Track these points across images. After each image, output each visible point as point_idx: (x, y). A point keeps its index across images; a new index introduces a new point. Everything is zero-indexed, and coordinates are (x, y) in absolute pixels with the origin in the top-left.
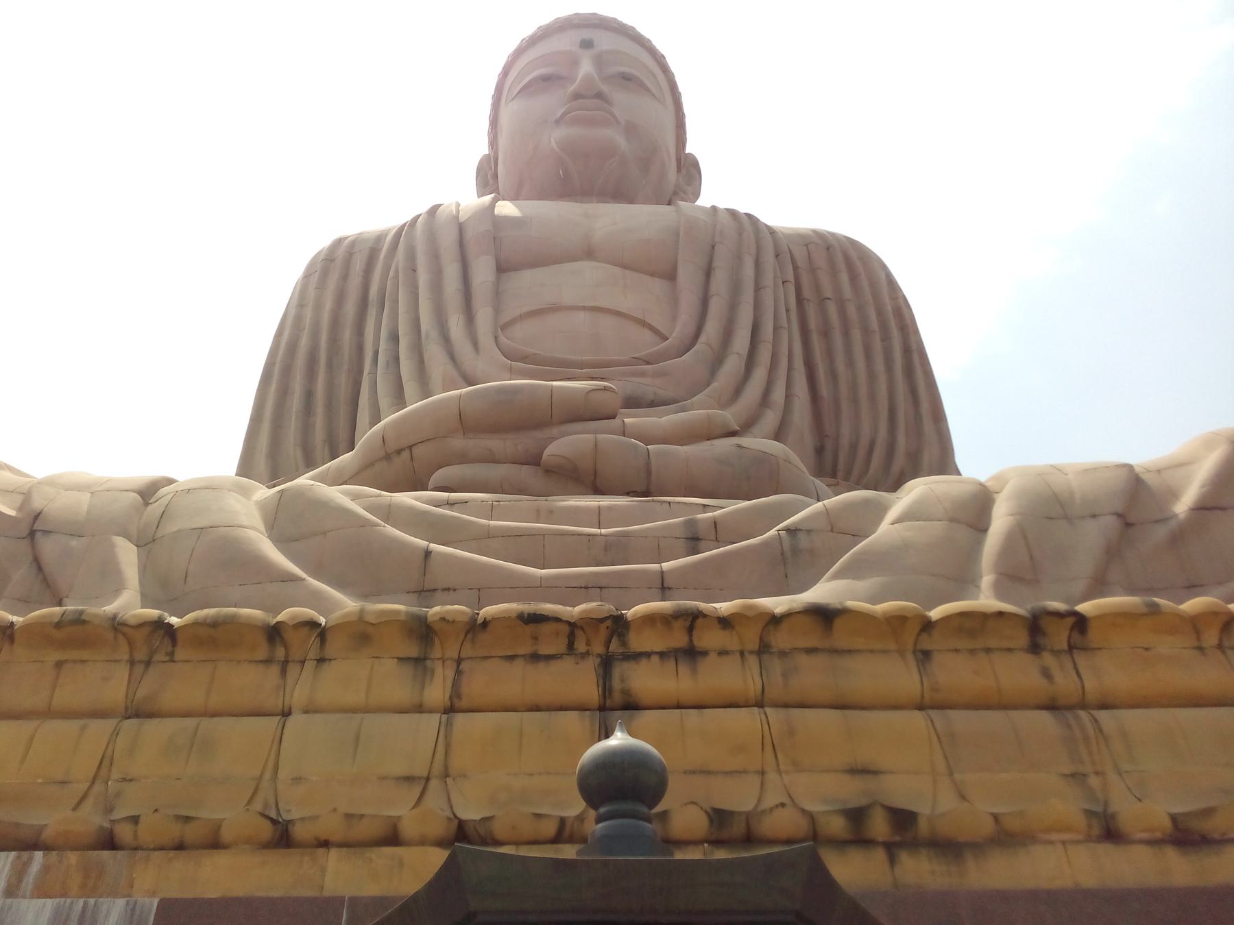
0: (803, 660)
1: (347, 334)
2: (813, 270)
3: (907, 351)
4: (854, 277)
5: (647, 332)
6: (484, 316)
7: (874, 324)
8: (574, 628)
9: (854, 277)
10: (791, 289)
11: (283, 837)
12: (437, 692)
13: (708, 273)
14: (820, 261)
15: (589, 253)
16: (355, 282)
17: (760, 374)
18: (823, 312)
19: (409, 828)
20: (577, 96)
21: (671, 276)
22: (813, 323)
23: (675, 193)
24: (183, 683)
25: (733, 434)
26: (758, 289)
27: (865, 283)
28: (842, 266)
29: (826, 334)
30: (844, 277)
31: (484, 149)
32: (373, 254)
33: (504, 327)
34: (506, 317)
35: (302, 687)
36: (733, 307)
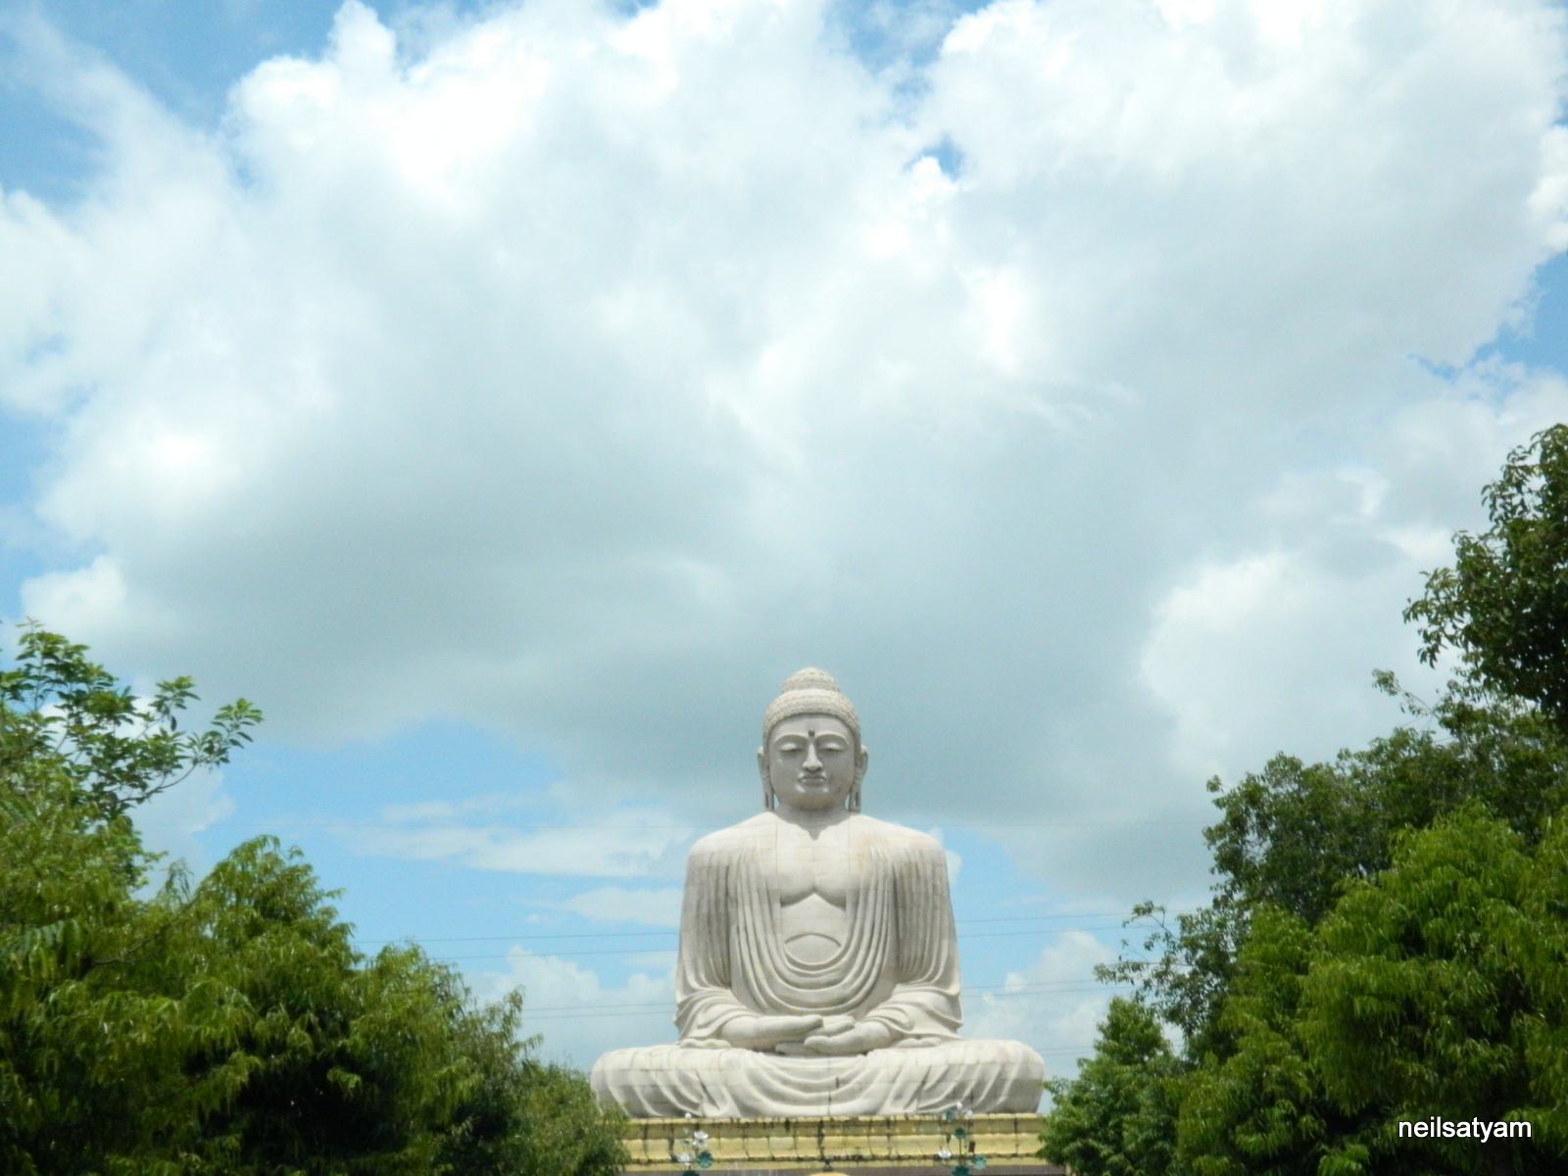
1: (722, 909)
2: (902, 877)
3: (935, 908)
4: (918, 877)
5: (834, 944)
6: (779, 935)
7: (922, 902)
9: (918, 877)
10: (891, 894)
11: (773, 1159)
14: (904, 872)
15: (814, 890)
16: (722, 882)
18: (904, 899)
22: (900, 905)
23: (854, 783)
27: (922, 879)
28: (914, 874)
29: (904, 908)
30: (914, 880)
32: (728, 868)
33: (787, 941)
34: (787, 938)
36: (864, 919)
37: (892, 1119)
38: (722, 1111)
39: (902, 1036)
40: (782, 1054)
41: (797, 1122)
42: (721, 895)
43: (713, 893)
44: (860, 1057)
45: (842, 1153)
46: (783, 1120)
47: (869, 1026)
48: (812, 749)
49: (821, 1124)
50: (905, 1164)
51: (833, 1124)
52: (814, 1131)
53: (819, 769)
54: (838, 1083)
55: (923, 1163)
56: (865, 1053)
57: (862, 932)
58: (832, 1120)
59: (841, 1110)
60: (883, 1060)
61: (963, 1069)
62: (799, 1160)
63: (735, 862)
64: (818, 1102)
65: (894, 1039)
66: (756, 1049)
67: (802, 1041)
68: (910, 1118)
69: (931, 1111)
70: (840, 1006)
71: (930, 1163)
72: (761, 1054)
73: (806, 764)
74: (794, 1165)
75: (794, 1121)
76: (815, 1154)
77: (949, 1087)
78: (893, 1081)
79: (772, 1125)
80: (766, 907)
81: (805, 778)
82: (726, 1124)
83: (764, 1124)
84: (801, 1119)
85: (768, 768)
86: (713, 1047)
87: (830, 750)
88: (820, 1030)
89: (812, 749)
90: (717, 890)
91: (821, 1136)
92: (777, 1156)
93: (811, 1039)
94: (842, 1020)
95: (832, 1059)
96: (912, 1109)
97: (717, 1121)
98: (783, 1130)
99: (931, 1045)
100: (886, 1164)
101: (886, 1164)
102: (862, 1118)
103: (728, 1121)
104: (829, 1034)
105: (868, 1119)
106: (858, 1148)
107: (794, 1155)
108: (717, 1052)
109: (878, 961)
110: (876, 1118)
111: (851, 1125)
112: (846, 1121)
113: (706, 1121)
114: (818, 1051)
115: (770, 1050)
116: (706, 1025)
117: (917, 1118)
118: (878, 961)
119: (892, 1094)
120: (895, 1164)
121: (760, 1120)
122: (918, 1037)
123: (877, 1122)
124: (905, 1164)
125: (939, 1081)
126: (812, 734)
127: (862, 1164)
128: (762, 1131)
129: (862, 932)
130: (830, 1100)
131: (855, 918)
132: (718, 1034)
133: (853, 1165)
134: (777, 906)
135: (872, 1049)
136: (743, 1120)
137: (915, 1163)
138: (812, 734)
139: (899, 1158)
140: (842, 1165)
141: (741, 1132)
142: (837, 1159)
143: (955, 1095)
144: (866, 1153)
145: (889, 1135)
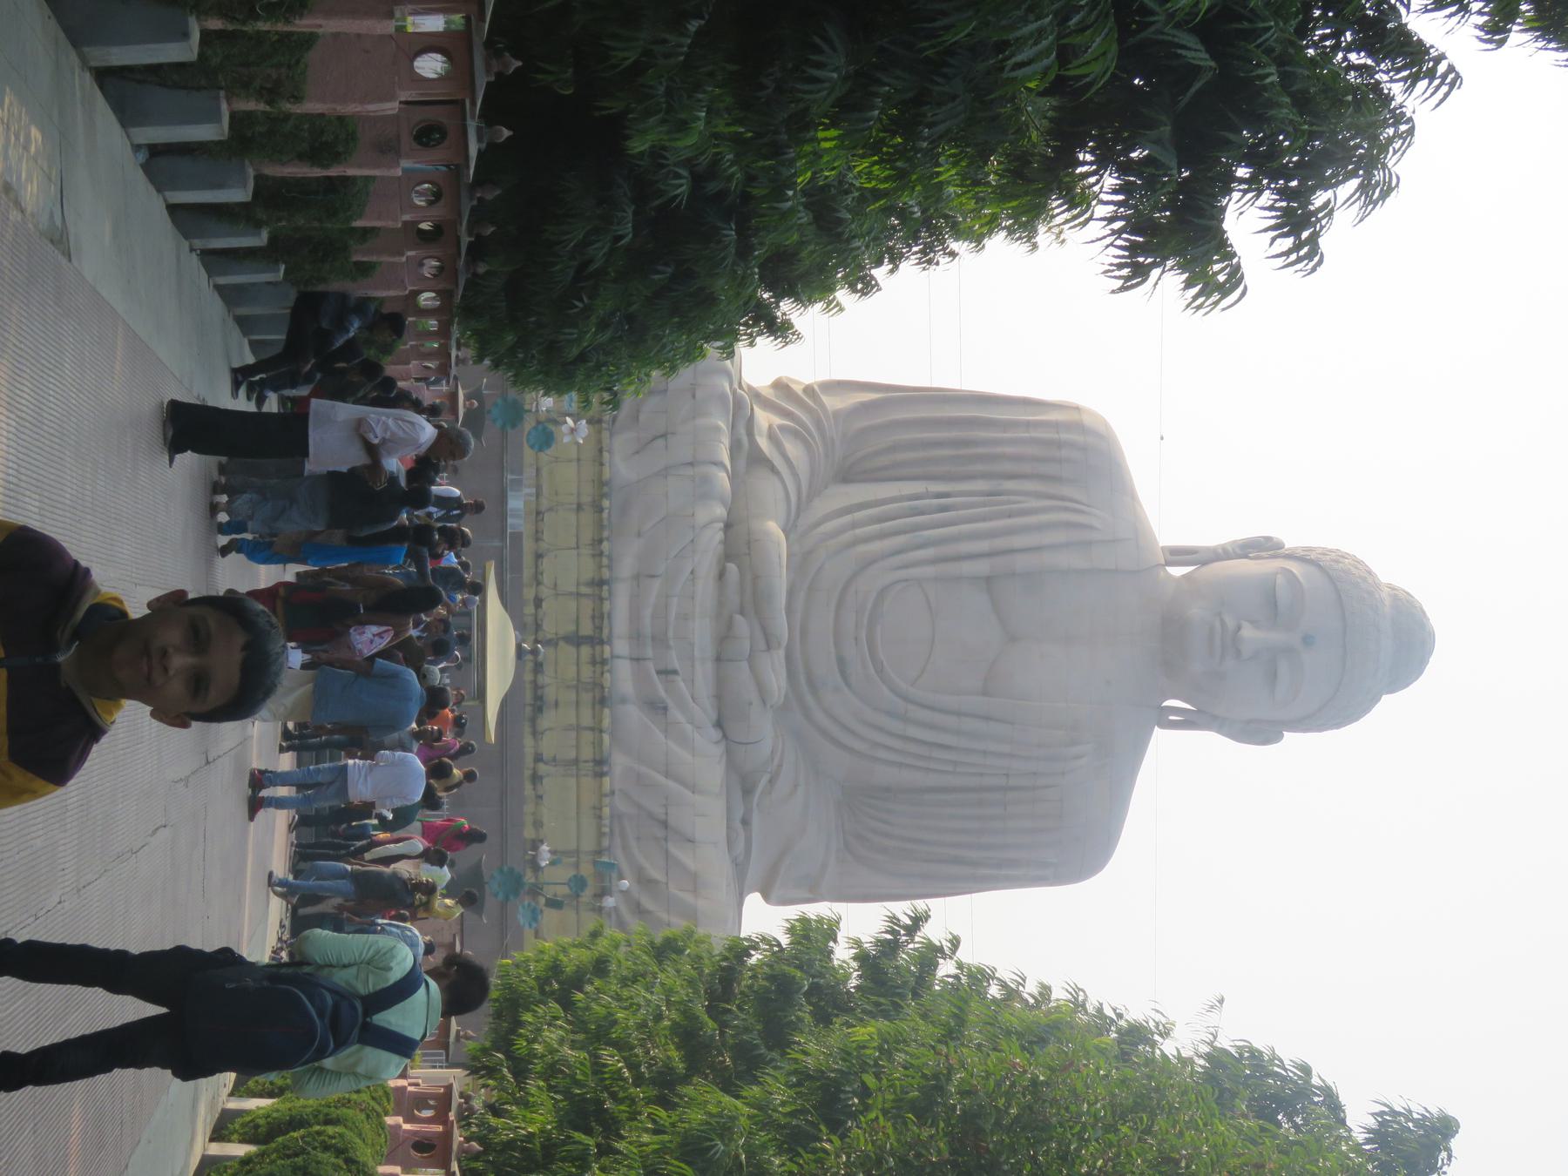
0: (590, 695)
1: (979, 467)
6: (930, 571)
8: (601, 629)
11: (539, 556)
12: (584, 590)
13: (987, 718)
17: (897, 744)
19: (542, 588)
20: (1239, 628)
21: (985, 693)
24: (588, 517)
25: (764, 702)
26: (985, 753)
31: (1291, 542)
35: (586, 551)
37: (605, 769)
38: (622, 467)
39: (747, 792)
40: (721, 575)
41: (601, 599)
42: (1008, 467)
43: (1009, 450)
44: (714, 716)
45: (546, 679)
46: (606, 574)
47: (764, 733)
48: (1276, 637)
49: (597, 640)
50: (528, 789)
51: (600, 663)
52: (587, 629)
53: (1238, 653)
54: (666, 673)
55: (529, 819)
56: (719, 725)
57: (932, 727)
58: (604, 662)
59: (623, 677)
60: (705, 761)
61: (688, 897)
62: (538, 602)
63: (1066, 491)
64: (636, 637)
65: (743, 783)
66: (728, 526)
67: (742, 612)
68: (606, 801)
69: (618, 840)
70: (802, 679)
71: (529, 833)
72: (720, 536)
73: (1248, 632)
74: (529, 593)
75: (605, 594)
76: (549, 629)
77: (656, 874)
78: (667, 775)
79: (601, 554)
80: (983, 546)
81: (1223, 623)
82: (601, 473)
83: (601, 541)
84: (606, 606)
85: (1246, 557)
86: (735, 448)
87: (1275, 675)
88: (762, 645)
89: (1276, 637)
90: (1017, 458)
91: (576, 640)
92: (546, 563)
93: (742, 625)
94: (777, 682)
95: (709, 666)
96: (622, 805)
97: (606, 455)
98: (588, 575)
99: (730, 843)
100: (529, 760)
101: (529, 760)
102: (607, 711)
103: (607, 475)
104: (751, 659)
105: (606, 722)
106: (557, 704)
107: (545, 592)
108: (725, 458)
109: (882, 754)
110: (606, 738)
111: (602, 701)
112: (603, 687)
113: (605, 434)
114: (724, 636)
115: (729, 554)
116: (771, 436)
117: (606, 811)
118: (882, 754)
119: (643, 769)
120: (528, 773)
121: (606, 534)
122: (745, 822)
123: (601, 740)
124: (528, 789)
125: (667, 851)
126: (1307, 640)
127: (528, 710)
128: (587, 535)
129: (932, 727)
130: (637, 660)
131: (959, 714)
132: (758, 459)
133: (528, 696)
134: (982, 567)
135: (725, 736)
136: (606, 503)
137: (529, 808)
138: (1307, 640)
139: (536, 778)
140: (528, 677)
141: (586, 499)
142: (538, 668)
143: (644, 881)
144: (547, 720)
145: (576, 761)
